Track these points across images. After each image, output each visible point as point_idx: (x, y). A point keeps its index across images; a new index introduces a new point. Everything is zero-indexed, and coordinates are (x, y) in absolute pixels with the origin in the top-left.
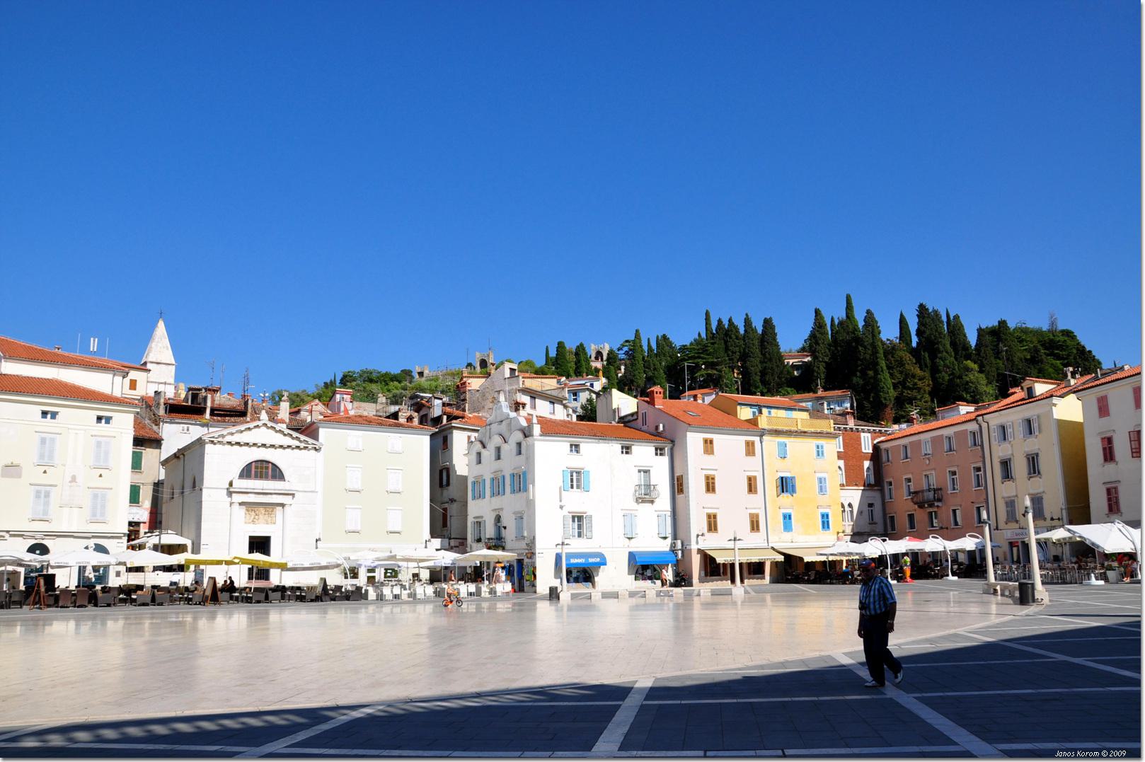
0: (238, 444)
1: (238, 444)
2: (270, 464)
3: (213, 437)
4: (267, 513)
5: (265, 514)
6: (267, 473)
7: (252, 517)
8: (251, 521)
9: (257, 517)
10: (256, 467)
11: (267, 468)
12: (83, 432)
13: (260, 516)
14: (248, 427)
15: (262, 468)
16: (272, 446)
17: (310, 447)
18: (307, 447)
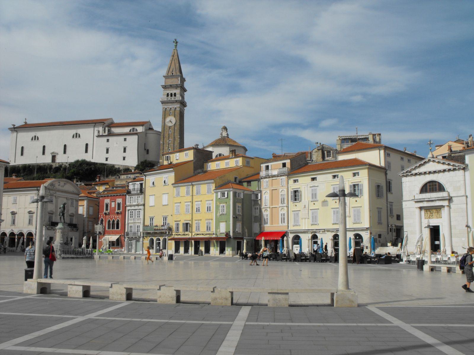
0: (416, 174)
1: (416, 174)
2: (437, 183)
3: (404, 173)
4: (436, 212)
5: (435, 213)
6: (436, 188)
7: (429, 216)
8: (428, 217)
9: (431, 214)
10: (430, 186)
11: (436, 185)
12: (348, 182)
13: (434, 214)
14: (420, 163)
15: (433, 186)
16: (435, 172)
17: (457, 168)
18: (455, 169)
